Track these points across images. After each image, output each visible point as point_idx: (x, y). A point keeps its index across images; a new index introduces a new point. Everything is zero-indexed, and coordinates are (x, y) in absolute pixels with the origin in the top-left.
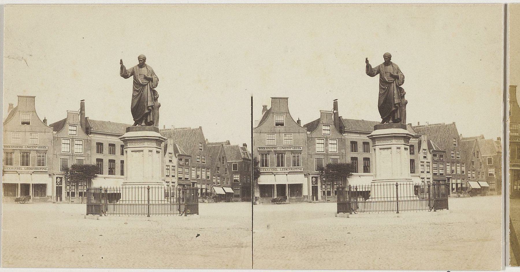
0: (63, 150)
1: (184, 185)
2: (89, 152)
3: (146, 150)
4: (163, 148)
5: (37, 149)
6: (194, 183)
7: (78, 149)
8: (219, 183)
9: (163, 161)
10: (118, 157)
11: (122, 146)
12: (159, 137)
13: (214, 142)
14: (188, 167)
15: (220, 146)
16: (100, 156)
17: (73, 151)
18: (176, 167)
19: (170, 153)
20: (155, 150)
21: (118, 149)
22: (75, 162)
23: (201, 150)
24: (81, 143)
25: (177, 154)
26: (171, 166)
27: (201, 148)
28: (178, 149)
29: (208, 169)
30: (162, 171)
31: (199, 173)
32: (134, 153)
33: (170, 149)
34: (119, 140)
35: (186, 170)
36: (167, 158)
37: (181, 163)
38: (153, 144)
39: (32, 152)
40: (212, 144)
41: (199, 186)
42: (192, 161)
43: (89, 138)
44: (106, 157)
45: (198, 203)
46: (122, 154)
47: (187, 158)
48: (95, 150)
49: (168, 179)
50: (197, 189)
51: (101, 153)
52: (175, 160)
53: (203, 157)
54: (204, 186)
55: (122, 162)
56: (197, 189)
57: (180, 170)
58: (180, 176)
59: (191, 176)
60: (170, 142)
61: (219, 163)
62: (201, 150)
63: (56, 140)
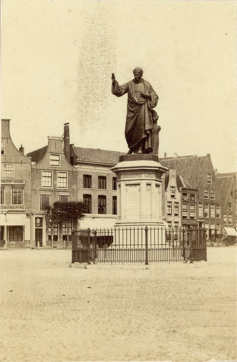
0: (43, 184)
1: (189, 226)
2: (74, 187)
3: (143, 184)
4: (164, 181)
5: (12, 183)
6: (201, 223)
7: (62, 183)
8: (230, 223)
9: (163, 196)
10: (109, 193)
11: (115, 179)
12: (159, 168)
13: (225, 172)
14: (193, 203)
15: (231, 178)
16: (87, 191)
17: (55, 186)
18: (180, 204)
19: (172, 187)
20: (154, 183)
21: (109, 183)
22: (58, 199)
23: (210, 182)
24: (65, 175)
25: (181, 188)
26: (173, 203)
27: (209, 180)
28: (183, 182)
29: (218, 205)
30: (163, 208)
31: (207, 210)
32: (128, 187)
33: (173, 182)
34: (111, 172)
35: (192, 208)
36: (169, 194)
37: (186, 198)
38: (152, 175)
39: (6, 187)
40: (223, 175)
41: (207, 226)
42: (198, 196)
43: (74, 170)
44: (95, 192)
45: (206, 246)
46: (115, 188)
47: (194, 192)
48: (82, 185)
49: (170, 219)
50: (205, 230)
51: (88, 187)
52: (178, 195)
53: (212, 192)
54: (213, 227)
55: (115, 198)
56: (205, 230)
57: (185, 207)
58: (185, 214)
59: (197, 213)
60: (172, 173)
61: (231, 197)
62: (210, 182)
63: (35, 173)
